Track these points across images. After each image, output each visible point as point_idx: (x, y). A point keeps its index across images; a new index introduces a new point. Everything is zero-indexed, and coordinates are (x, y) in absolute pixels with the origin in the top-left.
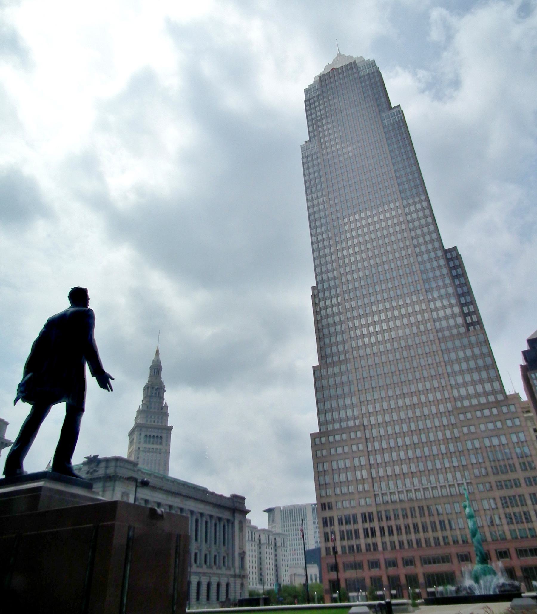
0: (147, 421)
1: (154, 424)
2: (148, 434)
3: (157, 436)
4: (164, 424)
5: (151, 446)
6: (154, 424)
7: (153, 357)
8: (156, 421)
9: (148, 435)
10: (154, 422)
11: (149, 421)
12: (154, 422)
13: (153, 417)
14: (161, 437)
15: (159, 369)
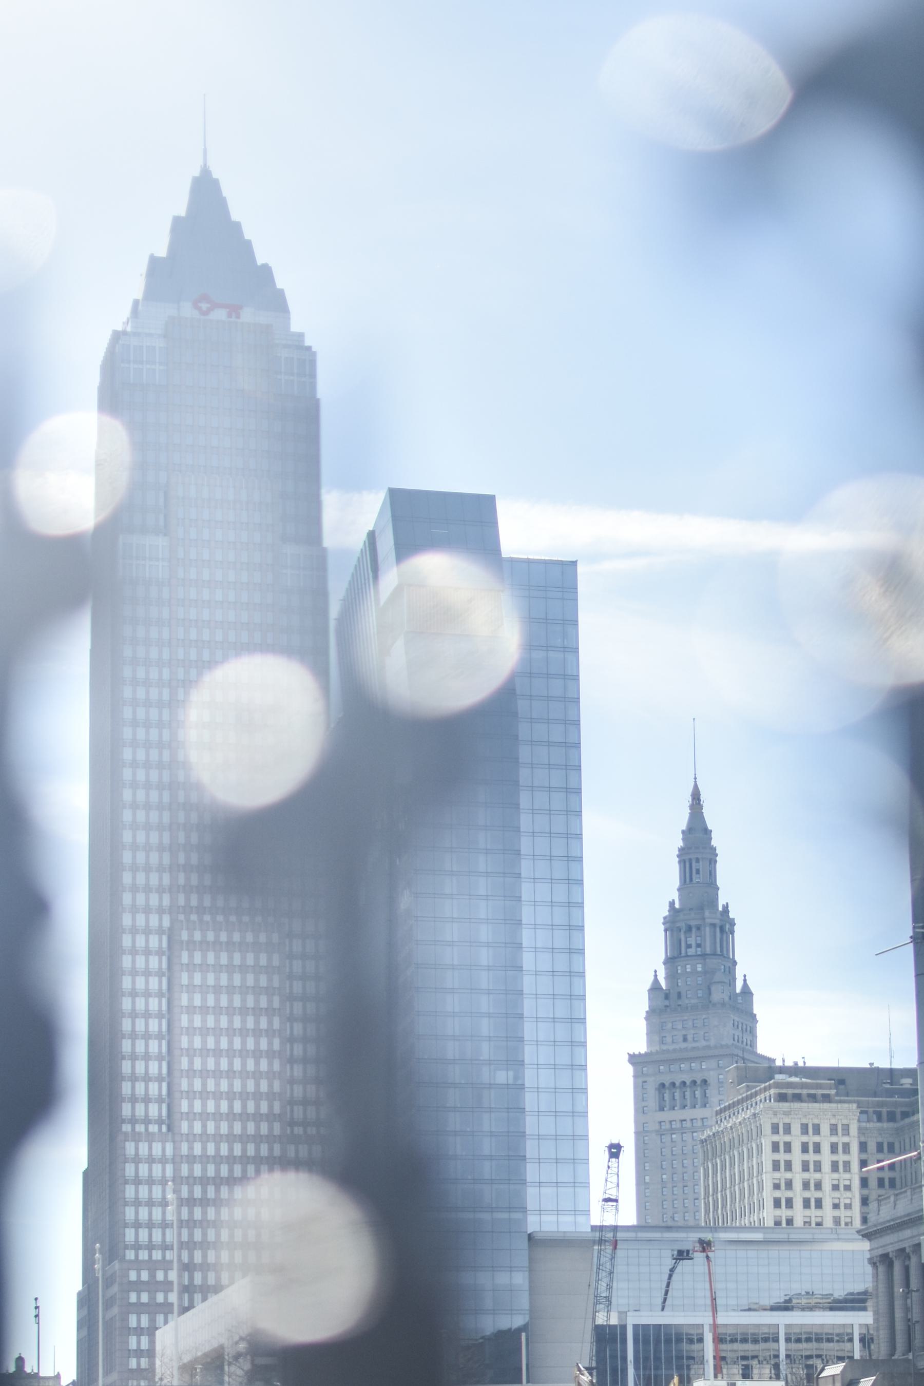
0: (662, 1042)
1: (684, 1045)
2: (667, 1080)
3: (694, 1082)
4: (712, 1042)
5: (678, 1114)
6: (684, 1045)
7: (682, 819)
8: (690, 1038)
9: (667, 1084)
10: (685, 1039)
11: (669, 1039)
12: (685, 1039)
13: (680, 1026)
14: (705, 1082)
15: (698, 860)
